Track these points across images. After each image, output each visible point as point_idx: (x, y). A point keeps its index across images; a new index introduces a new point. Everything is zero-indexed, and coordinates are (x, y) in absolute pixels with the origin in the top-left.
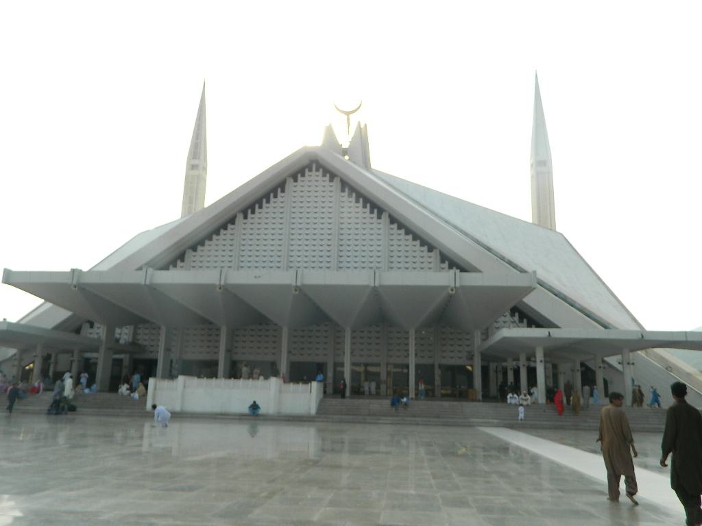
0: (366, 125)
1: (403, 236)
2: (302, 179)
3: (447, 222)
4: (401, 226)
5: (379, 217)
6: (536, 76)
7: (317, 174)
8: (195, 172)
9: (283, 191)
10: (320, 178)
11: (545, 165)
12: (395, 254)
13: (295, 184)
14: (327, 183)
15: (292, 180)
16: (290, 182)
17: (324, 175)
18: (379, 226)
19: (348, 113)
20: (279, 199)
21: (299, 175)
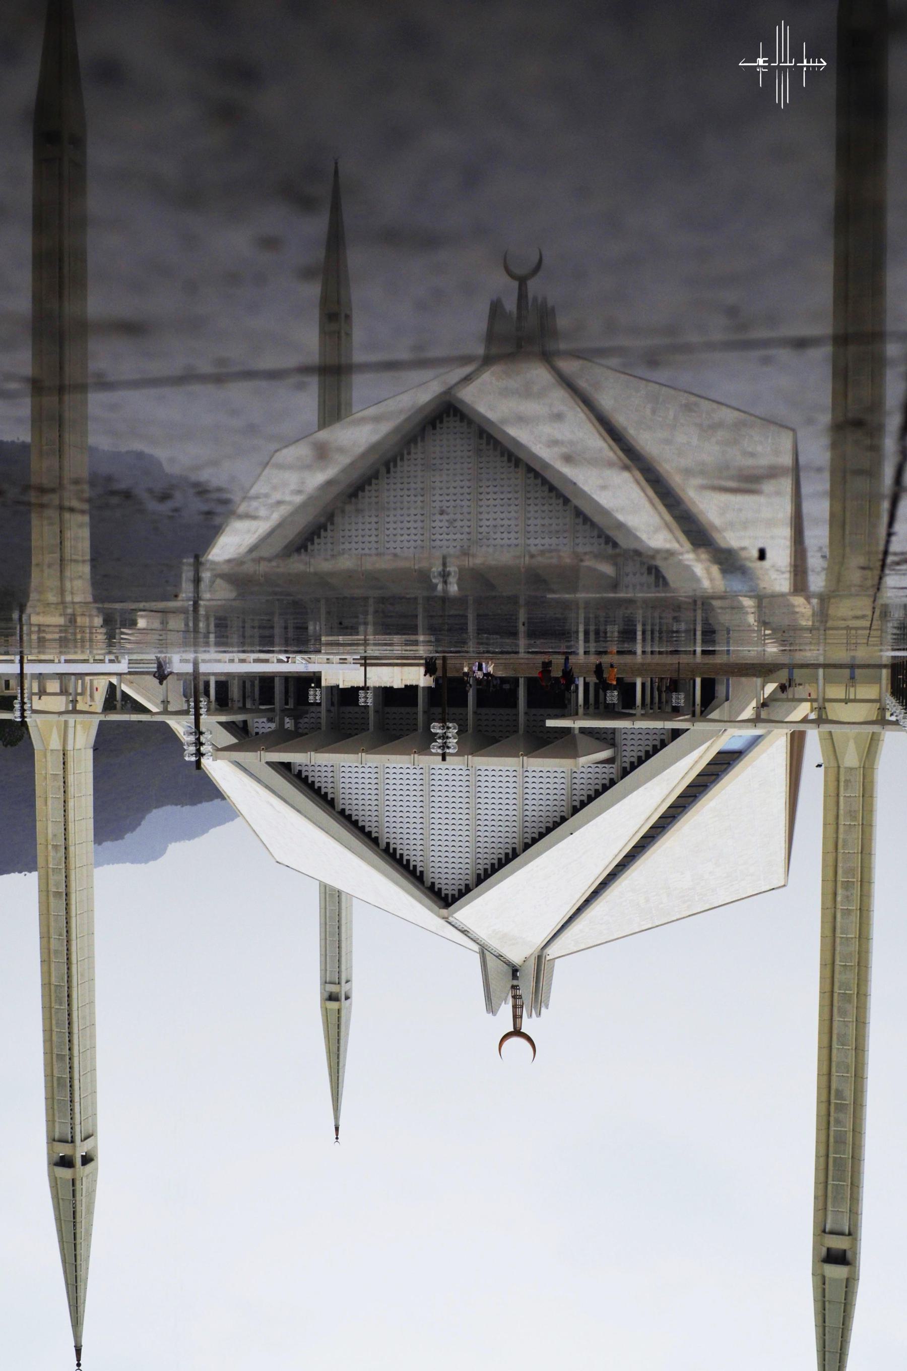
1: (367, 824)
2: (460, 887)
4: (368, 835)
7: (446, 892)
9: (479, 875)
10: (444, 887)
18: (388, 835)
19: (518, 1032)
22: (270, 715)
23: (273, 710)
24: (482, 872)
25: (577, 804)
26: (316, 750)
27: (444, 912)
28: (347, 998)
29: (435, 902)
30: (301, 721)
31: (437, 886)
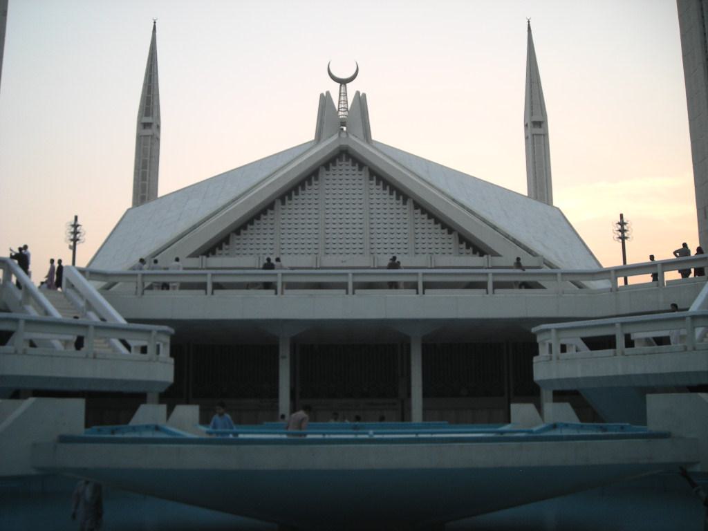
0: (364, 95)
1: (426, 220)
3: (454, 200)
6: (529, 25)
7: (347, 163)
8: (148, 132)
9: (317, 179)
10: (350, 167)
11: (540, 127)
12: (420, 236)
13: (327, 173)
14: (357, 172)
15: (324, 169)
16: (323, 170)
17: (353, 165)
19: (343, 82)
21: (331, 165)
24: (314, 182)
27: (343, 143)
31: (357, 167)
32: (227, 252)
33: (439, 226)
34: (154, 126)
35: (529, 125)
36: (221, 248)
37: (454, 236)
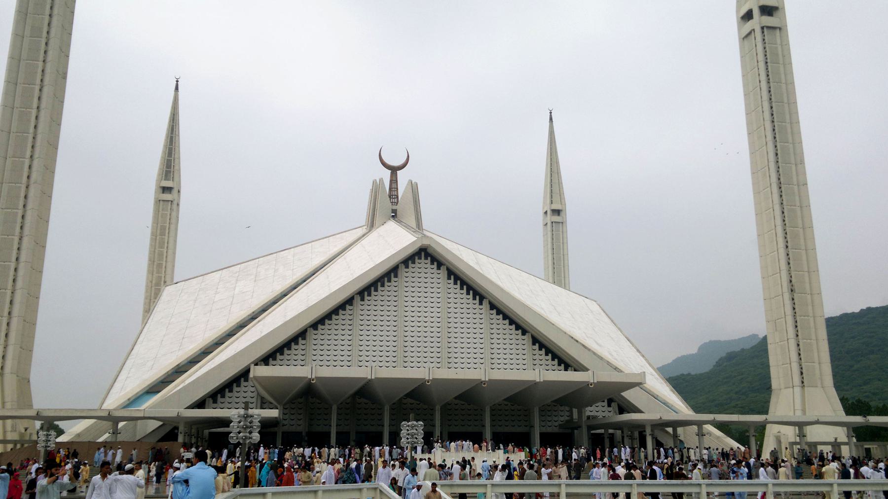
1: (501, 321)
2: (413, 265)
4: (499, 312)
5: (481, 303)
6: (551, 119)
7: (426, 261)
8: (167, 196)
9: (396, 276)
10: (429, 265)
11: (559, 215)
13: (407, 270)
14: (435, 270)
17: (432, 263)
18: (481, 312)
19: (394, 170)
20: (393, 283)
22: (592, 422)
23: (590, 428)
24: (393, 279)
25: (301, 341)
26: (535, 384)
27: (426, 242)
28: (546, 213)
29: (434, 250)
30: (567, 418)
32: (303, 347)
33: (513, 327)
34: (175, 191)
35: (549, 212)
36: (297, 343)
37: (527, 338)
